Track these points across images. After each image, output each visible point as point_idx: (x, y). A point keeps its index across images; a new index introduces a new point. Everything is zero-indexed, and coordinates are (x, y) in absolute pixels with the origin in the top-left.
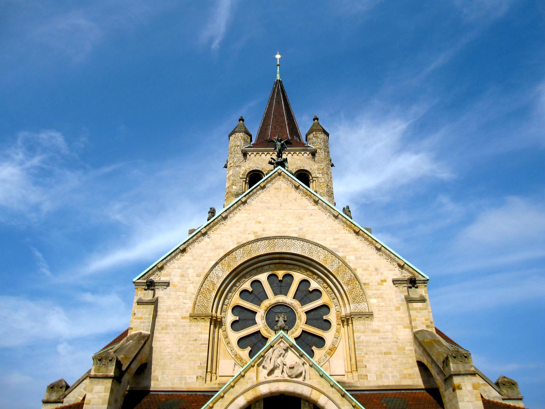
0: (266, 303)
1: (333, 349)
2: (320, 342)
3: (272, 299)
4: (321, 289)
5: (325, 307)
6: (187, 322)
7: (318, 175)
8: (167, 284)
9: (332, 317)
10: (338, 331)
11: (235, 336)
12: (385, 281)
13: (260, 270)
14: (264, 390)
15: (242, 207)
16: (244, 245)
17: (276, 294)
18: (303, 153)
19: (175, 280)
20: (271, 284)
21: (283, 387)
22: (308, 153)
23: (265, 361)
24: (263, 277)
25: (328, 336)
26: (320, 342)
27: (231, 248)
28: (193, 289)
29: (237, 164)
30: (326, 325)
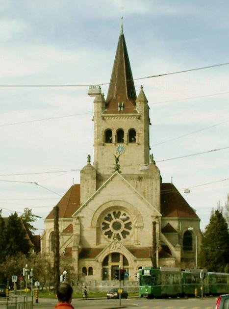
0: (113, 221)
1: (132, 236)
2: (128, 233)
3: (114, 220)
4: (129, 216)
5: (130, 223)
6: (90, 229)
7: (140, 132)
8: (83, 217)
9: (132, 226)
10: (134, 230)
11: (104, 232)
12: (148, 216)
13: (110, 210)
14: (111, 252)
15: (105, 188)
16: (106, 203)
17: (115, 218)
18: (133, 117)
19: (85, 216)
20: (114, 215)
21: (115, 251)
22: (135, 117)
23: (123, 180)
24: (112, 213)
25: (131, 232)
26: (128, 233)
27: (101, 204)
28: (91, 218)
29: (99, 124)
30: (130, 228)
